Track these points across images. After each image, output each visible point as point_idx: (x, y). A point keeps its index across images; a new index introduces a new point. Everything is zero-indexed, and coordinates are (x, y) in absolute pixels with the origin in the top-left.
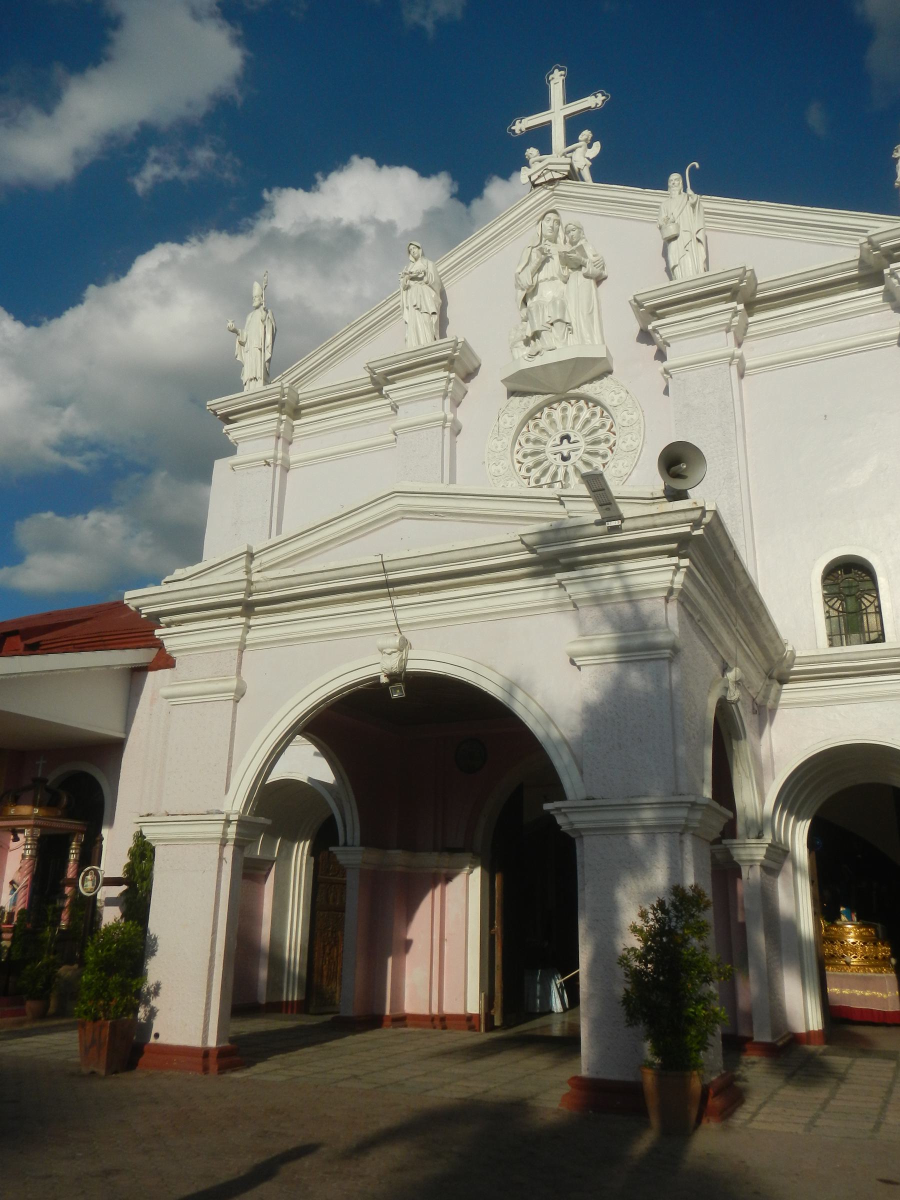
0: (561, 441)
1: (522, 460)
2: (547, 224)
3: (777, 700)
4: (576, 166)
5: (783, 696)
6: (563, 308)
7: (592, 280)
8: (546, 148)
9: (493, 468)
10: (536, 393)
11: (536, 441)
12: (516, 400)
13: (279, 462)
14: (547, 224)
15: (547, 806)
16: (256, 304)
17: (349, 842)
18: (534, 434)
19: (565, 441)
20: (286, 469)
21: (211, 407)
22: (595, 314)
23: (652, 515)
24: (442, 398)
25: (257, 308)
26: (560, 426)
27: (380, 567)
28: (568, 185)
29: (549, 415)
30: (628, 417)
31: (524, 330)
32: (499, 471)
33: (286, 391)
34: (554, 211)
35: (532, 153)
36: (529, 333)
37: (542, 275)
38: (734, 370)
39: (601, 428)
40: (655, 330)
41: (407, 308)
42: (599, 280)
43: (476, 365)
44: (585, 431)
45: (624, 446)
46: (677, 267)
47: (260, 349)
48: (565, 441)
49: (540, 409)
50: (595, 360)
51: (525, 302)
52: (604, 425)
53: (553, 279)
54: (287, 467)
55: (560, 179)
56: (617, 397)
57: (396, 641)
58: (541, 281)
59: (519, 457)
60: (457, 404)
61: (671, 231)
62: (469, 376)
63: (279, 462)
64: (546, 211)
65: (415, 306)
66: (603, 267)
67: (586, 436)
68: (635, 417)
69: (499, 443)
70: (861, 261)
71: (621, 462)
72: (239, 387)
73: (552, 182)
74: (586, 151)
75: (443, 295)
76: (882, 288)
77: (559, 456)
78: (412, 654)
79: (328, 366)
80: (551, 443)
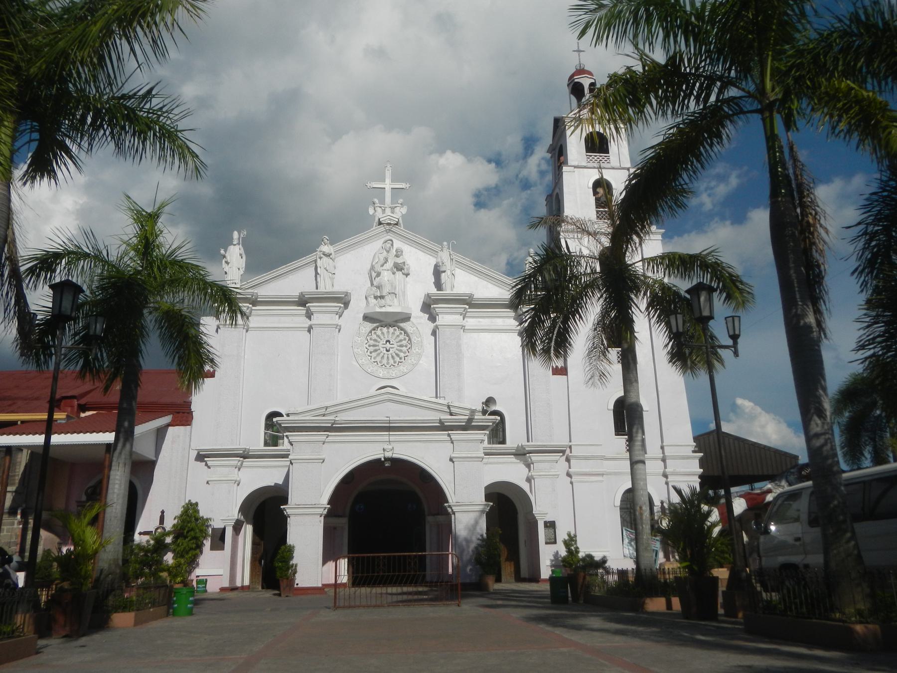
8: (382, 201)
13: (246, 327)
14: (388, 245)
18: (374, 337)
20: (247, 331)
25: (235, 245)
26: (386, 336)
36: (379, 295)
37: (384, 267)
40: (434, 308)
41: (320, 267)
42: (407, 275)
45: (414, 351)
47: (239, 269)
56: (412, 329)
59: (367, 346)
60: (340, 316)
62: (346, 305)
67: (397, 342)
71: (413, 358)
73: (389, 224)
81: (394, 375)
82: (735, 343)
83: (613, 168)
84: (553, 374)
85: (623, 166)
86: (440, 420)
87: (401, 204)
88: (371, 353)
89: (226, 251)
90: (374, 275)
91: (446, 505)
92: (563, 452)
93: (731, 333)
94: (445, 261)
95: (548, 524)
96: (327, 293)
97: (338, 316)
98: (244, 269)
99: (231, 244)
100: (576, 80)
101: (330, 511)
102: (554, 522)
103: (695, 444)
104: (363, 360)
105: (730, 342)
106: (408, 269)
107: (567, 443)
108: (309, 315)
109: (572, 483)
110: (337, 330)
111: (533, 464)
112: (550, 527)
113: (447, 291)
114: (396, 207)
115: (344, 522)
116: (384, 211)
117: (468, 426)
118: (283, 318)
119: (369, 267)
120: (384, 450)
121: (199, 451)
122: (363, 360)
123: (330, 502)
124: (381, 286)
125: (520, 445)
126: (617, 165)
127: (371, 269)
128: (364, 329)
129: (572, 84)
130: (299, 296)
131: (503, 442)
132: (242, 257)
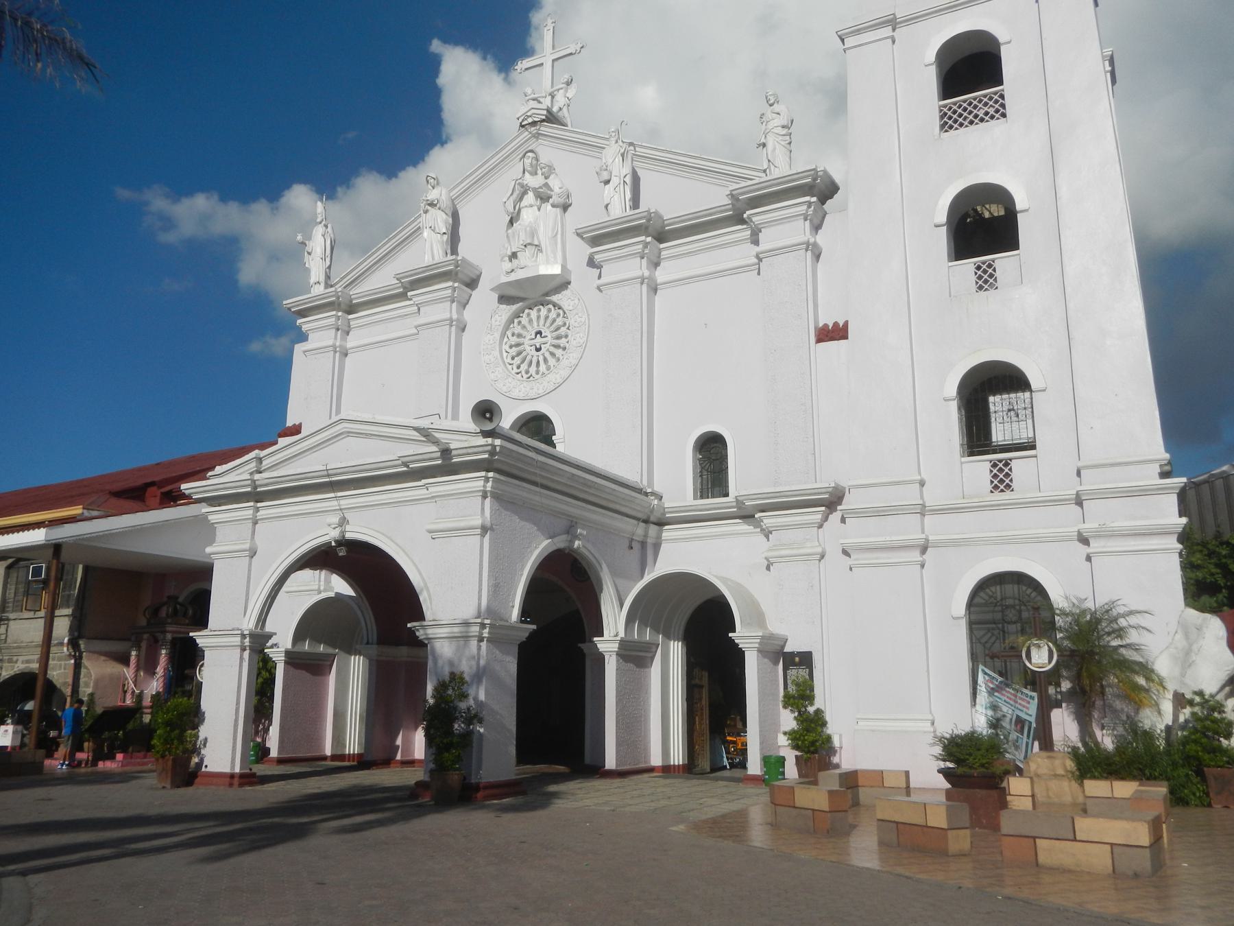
0: (536, 337)
1: (509, 350)
2: (528, 161)
3: (659, 537)
4: (555, 109)
5: (663, 534)
6: (533, 233)
7: (558, 209)
11: (519, 336)
13: (338, 349)
14: (528, 161)
15: (409, 625)
16: (319, 220)
17: (370, 641)
18: (518, 330)
19: (538, 335)
21: (288, 306)
22: (559, 236)
23: (466, 448)
24: (449, 303)
25: (320, 223)
26: (535, 323)
27: (325, 473)
28: (546, 126)
29: (529, 315)
30: (579, 320)
31: (507, 249)
32: (490, 360)
34: (531, 151)
36: (509, 253)
37: (524, 203)
39: (563, 326)
42: (565, 207)
43: (478, 273)
44: (552, 328)
46: (609, 205)
47: (322, 259)
48: (538, 335)
50: (553, 277)
51: (511, 222)
52: (565, 324)
54: (345, 352)
55: (539, 121)
56: (572, 303)
57: (335, 519)
58: (523, 208)
59: (506, 347)
60: (464, 305)
61: (605, 176)
64: (525, 151)
65: (431, 227)
66: (568, 196)
68: (583, 320)
69: (492, 337)
71: (571, 355)
73: (534, 124)
74: (566, 91)
75: (455, 216)
77: (533, 348)
78: (348, 528)
79: (374, 271)
80: (529, 337)
81: (540, 392)
84: (819, 340)
88: (513, 358)
95: (797, 659)
102: (810, 654)
103: (1167, 456)
112: (800, 664)
114: (558, 90)
117: (447, 465)
131: (727, 495)
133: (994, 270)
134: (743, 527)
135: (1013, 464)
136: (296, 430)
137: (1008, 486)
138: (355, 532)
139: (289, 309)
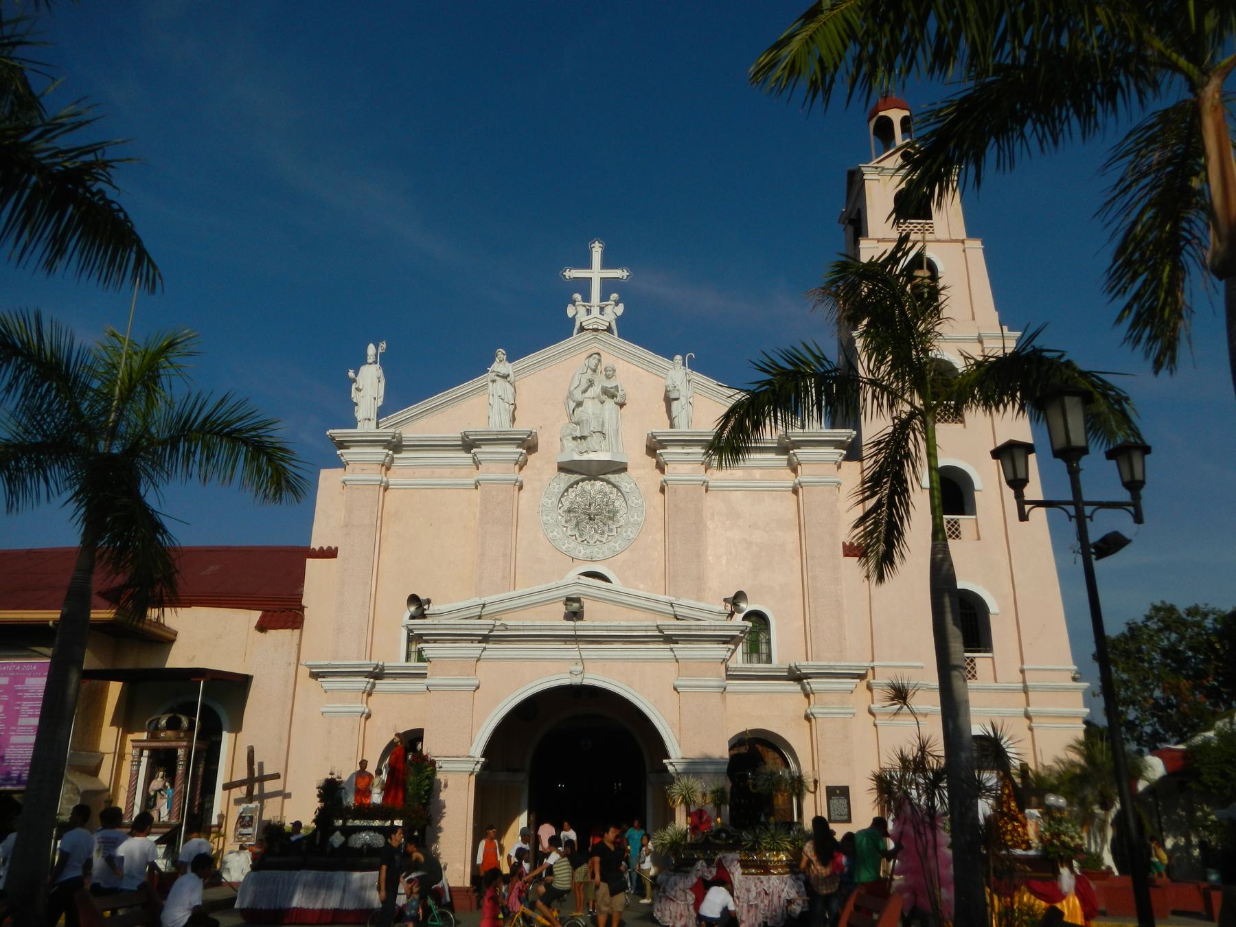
8: (587, 298)
9: (544, 518)
10: (576, 473)
12: (563, 475)
13: (383, 484)
14: (593, 362)
20: (386, 489)
21: (333, 435)
25: (371, 364)
30: (636, 501)
33: (397, 435)
34: (598, 354)
35: (577, 296)
36: (579, 436)
37: (587, 394)
38: (704, 488)
40: (660, 454)
42: (622, 405)
45: (632, 520)
49: (577, 483)
53: (593, 398)
56: (629, 486)
60: (521, 469)
63: (383, 484)
69: (550, 501)
70: (779, 440)
72: (353, 423)
73: (596, 330)
76: (786, 457)
78: (586, 675)
82: (1136, 498)
83: (939, 241)
84: (846, 555)
85: (953, 237)
86: (657, 626)
87: (615, 301)
89: (356, 373)
90: (572, 405)
91: (664, 761)
92: (861, 677)
93: (1127, 478)
94: (678, 383)
96: (500, 432)
97: (517, 466)
98: (382, 399)
99: (365, 362)
100: (881, 114)
101: (485, 767)
103: (1075, 667)
104: (555, 533)
105: (1125, 496)
106: (624, 397)
107: (867, 664)
108: (477, 464)
109: (875, 725)
110: (517, 488)
111: (813, 694)
113: (682, 427)
115: (522, 778)
116: (589, 312)
118: (438, 471)
119: (566, 393)
120: (571, 673)
121: (310, 667)
122: (555, 533)
123: (485, 754)
124: (582, 421)
125: (793, 665)
126: (946, 236)
127: (568, 397)
128: (557, 486)
129: (874, 120)
130: (462, 437)
131: (769, 660)
132: (379, 381)
133: (959, 526)
134: (794, 687)
135: (977, 661)
136: (331, 553)
137: (973, 676)
138: (594, 678)
139: (333, 438)
